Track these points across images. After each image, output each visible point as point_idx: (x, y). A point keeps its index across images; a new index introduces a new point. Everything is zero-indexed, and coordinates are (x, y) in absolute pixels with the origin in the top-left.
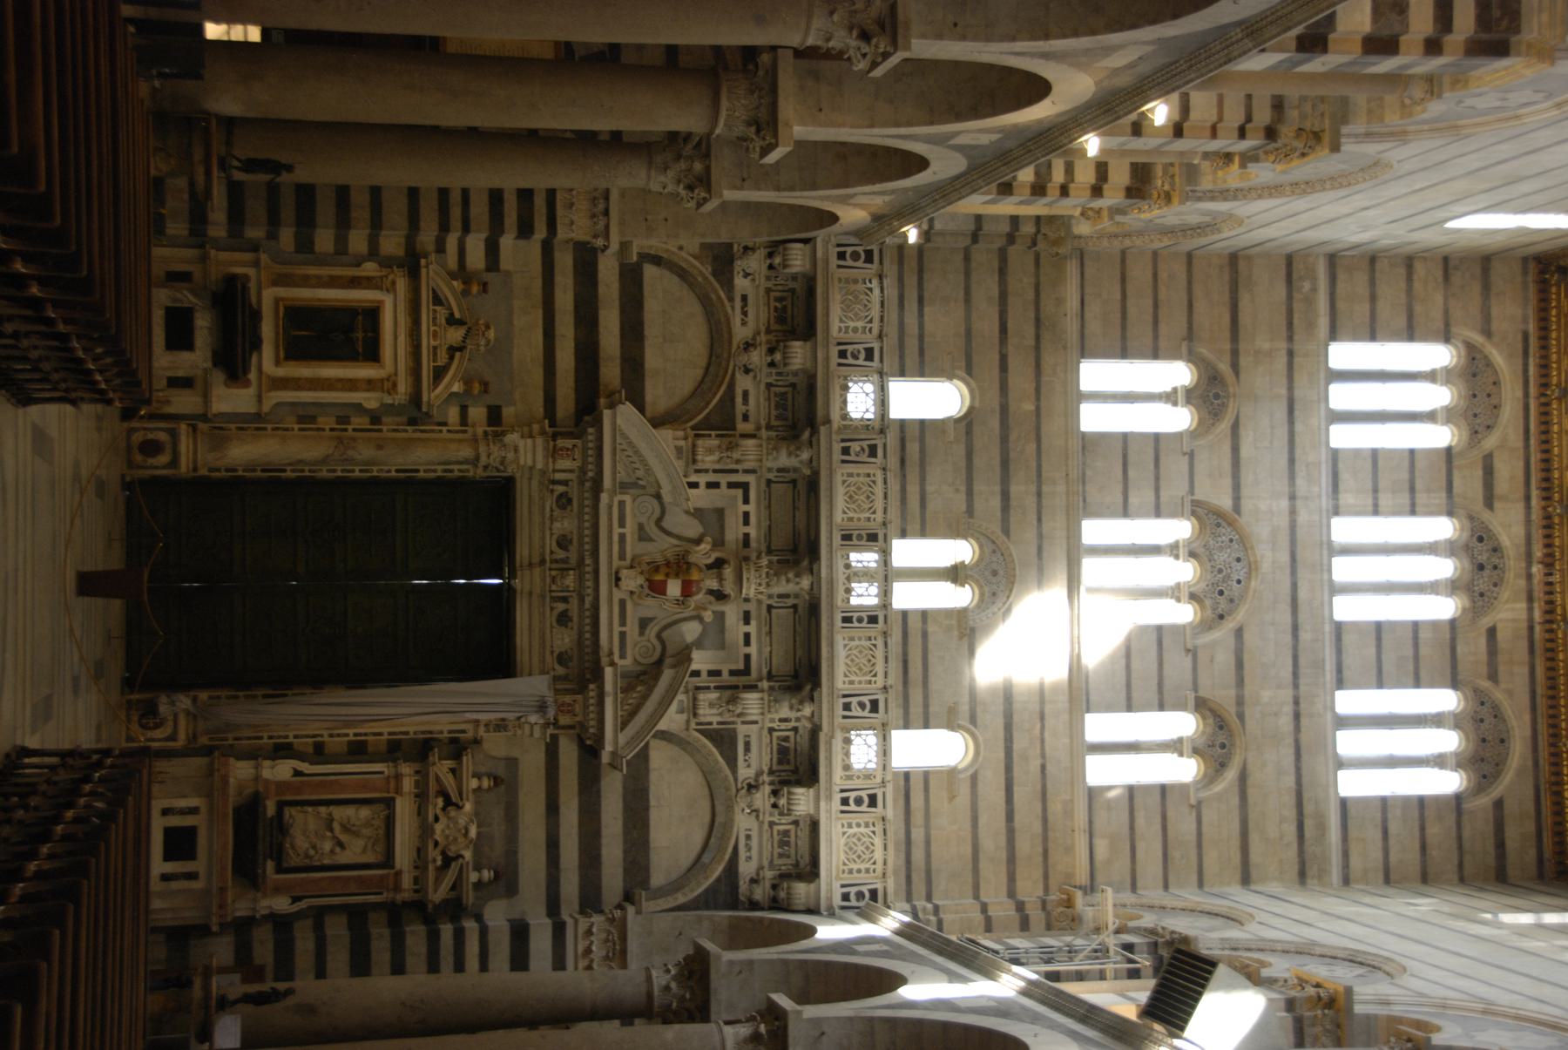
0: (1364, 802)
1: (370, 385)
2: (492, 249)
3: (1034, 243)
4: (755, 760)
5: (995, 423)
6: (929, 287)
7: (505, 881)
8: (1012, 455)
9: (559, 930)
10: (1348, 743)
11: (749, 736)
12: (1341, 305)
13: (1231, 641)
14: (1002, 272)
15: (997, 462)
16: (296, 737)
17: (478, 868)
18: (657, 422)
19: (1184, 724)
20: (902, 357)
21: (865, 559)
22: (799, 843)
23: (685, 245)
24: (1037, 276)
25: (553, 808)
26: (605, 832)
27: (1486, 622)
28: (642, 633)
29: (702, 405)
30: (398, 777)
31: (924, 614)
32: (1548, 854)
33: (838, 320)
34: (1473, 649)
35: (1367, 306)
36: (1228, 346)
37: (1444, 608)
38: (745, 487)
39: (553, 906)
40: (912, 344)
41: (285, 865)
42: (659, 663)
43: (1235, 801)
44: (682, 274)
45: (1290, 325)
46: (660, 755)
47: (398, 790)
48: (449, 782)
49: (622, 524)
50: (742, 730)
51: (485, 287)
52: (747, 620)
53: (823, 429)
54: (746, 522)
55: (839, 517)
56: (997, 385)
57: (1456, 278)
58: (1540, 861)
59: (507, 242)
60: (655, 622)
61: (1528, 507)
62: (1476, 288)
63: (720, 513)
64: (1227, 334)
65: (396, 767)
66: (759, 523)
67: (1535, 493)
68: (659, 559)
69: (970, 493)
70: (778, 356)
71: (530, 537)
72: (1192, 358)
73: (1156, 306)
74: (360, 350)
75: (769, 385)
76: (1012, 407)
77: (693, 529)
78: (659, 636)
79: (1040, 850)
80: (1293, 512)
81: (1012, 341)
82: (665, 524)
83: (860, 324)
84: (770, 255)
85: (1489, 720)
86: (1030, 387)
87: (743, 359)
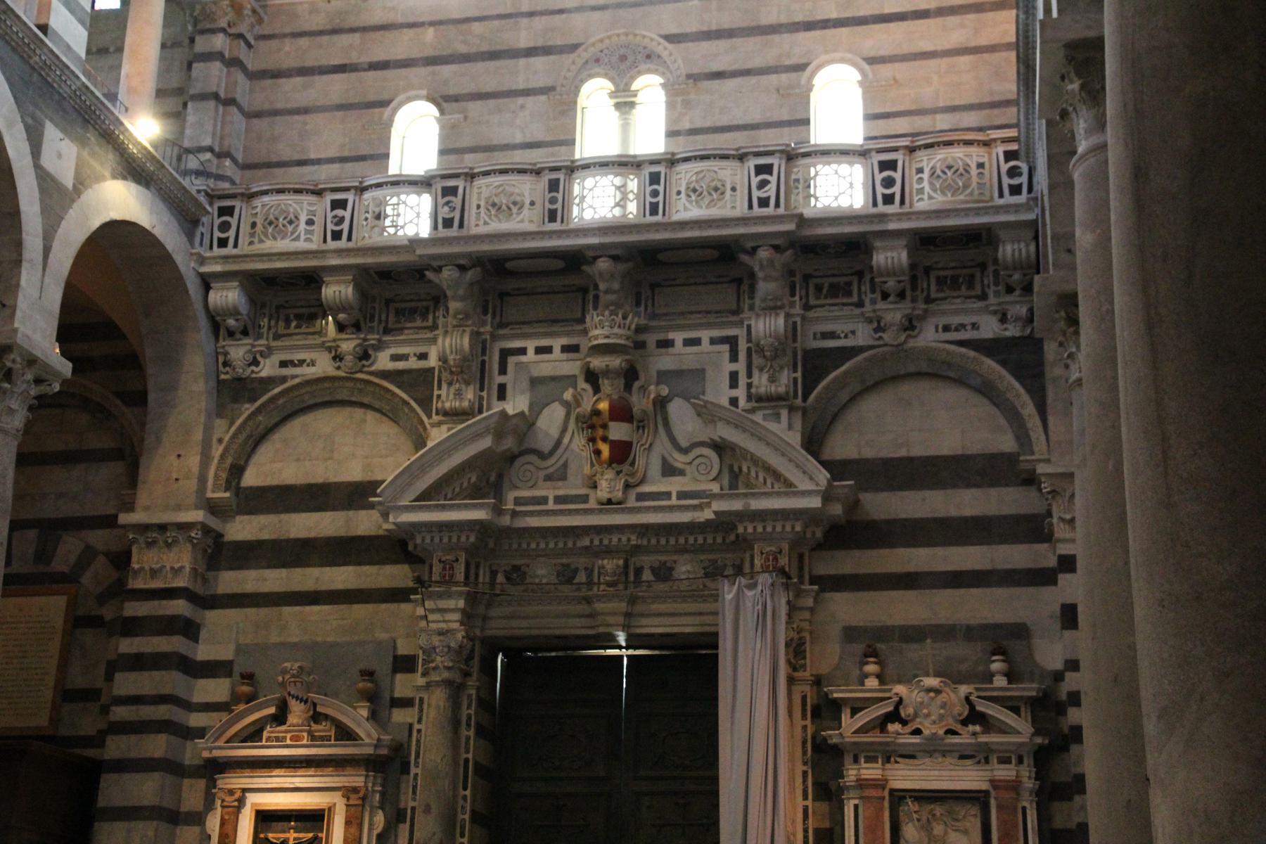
5: (446, 70)
6: (287, 154)
11: (815, 334)
15: (492, 65)
22: (952, 264)
26: (941, 512)
28: (682, 473)
29: (406, 410)
30: (862, 784)
47: (880, 784)
49: (544, 500)
51: (248, 677)
52: (666, 344)
54: (548, 350)
56: (403, 72)
59: (204, 652)
60: (667, 456)
65: (848, 788)
68: (587, 453)
69: (527, 93)
71: (558, 616)
74: (311, 835)
75: (387, 331)
76: (430, 52)
78: (685, 451)
81: (354, 58)
82: (546, 449)
86: (408, 34)
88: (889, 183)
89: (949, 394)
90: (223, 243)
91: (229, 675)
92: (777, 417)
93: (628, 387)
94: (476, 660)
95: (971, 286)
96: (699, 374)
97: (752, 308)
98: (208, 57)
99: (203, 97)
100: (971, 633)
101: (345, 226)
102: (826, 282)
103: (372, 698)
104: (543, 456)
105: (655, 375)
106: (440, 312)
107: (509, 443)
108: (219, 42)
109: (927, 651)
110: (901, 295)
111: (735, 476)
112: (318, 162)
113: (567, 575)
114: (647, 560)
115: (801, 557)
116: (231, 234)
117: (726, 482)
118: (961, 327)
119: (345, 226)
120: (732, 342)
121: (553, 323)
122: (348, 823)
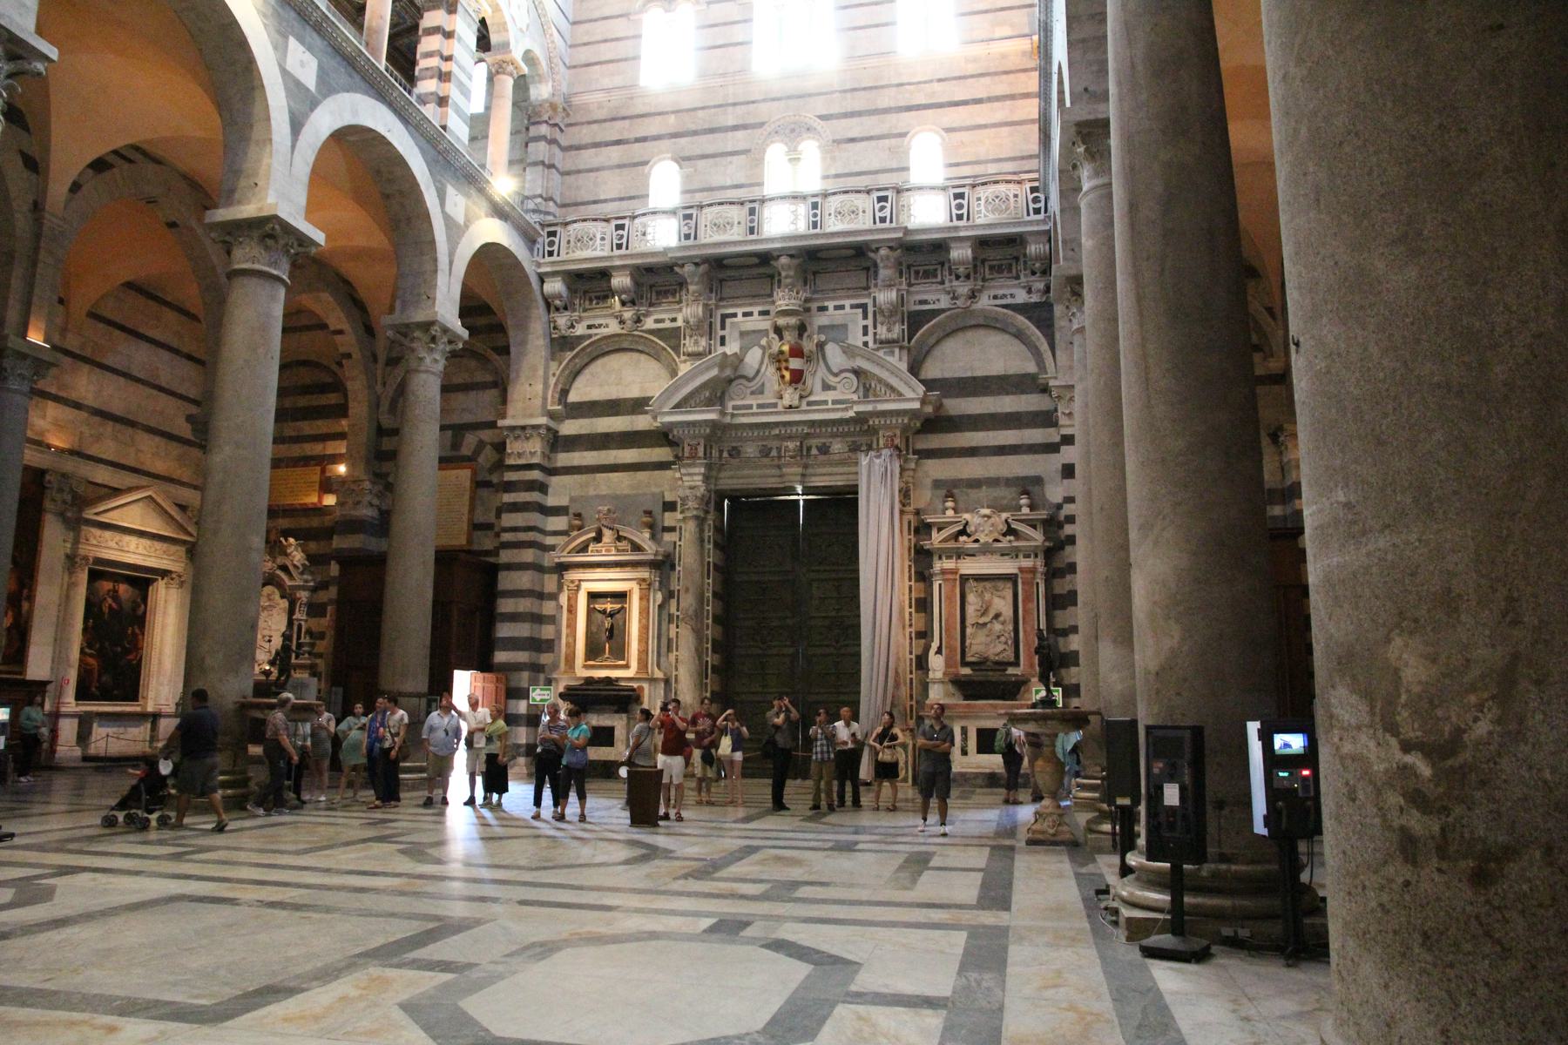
1: (644, 598)
3: (556, 125)
4: (935, 297)
5: (683, 141)
7: (1029, 486)
8: (706, 126)
14: (578, 148)
15: (710, 136)
16: (911, 653)
24: (582, 124)
26: (992, 410)
30: (944, 572)
41: (1012, 659)
46: (932, 370)
47: (954, 572)
48: (945, 533)
49: (750, 407)
51: (578, 515)
52: (823, 309)
59: (551, 501)
66: (751, 305)
68: (776, 378)
73: (606, 41)
75: (651, 305)
76: (672, 130)
78: (836, 375)
79: (1004, 77)
81: (626, 136)
88: (960, 207)
89: (995, 338)
90: (551, 254)
91: (567, 514)
92: (892, 353)
93: (801, 336)
94: (713, 503)
95: (1010, 270)
96: (844, 327)
97: (876, 285)
98: (537, 139)
99: (535, 164)
100: (1009, 482)
101: (624, 241)
102: (921, 269)
103: (651, 526)
104: (749, 380)
105: (816, 327)
106: (684, 292)
107: (728, 372)
108: (544, 129)
109: (984, 493)
110: (968, 277)
111: (867, 390)
112: (605, 201)
113: (765, 453)
114: (814, 442)
115: (907, 440)
116: (555, 248)
117: (861, 394)
118: (1004, 296)
119: (624, 241)
120: (864, 307)
121: (754, 297)
122: (641, 599)
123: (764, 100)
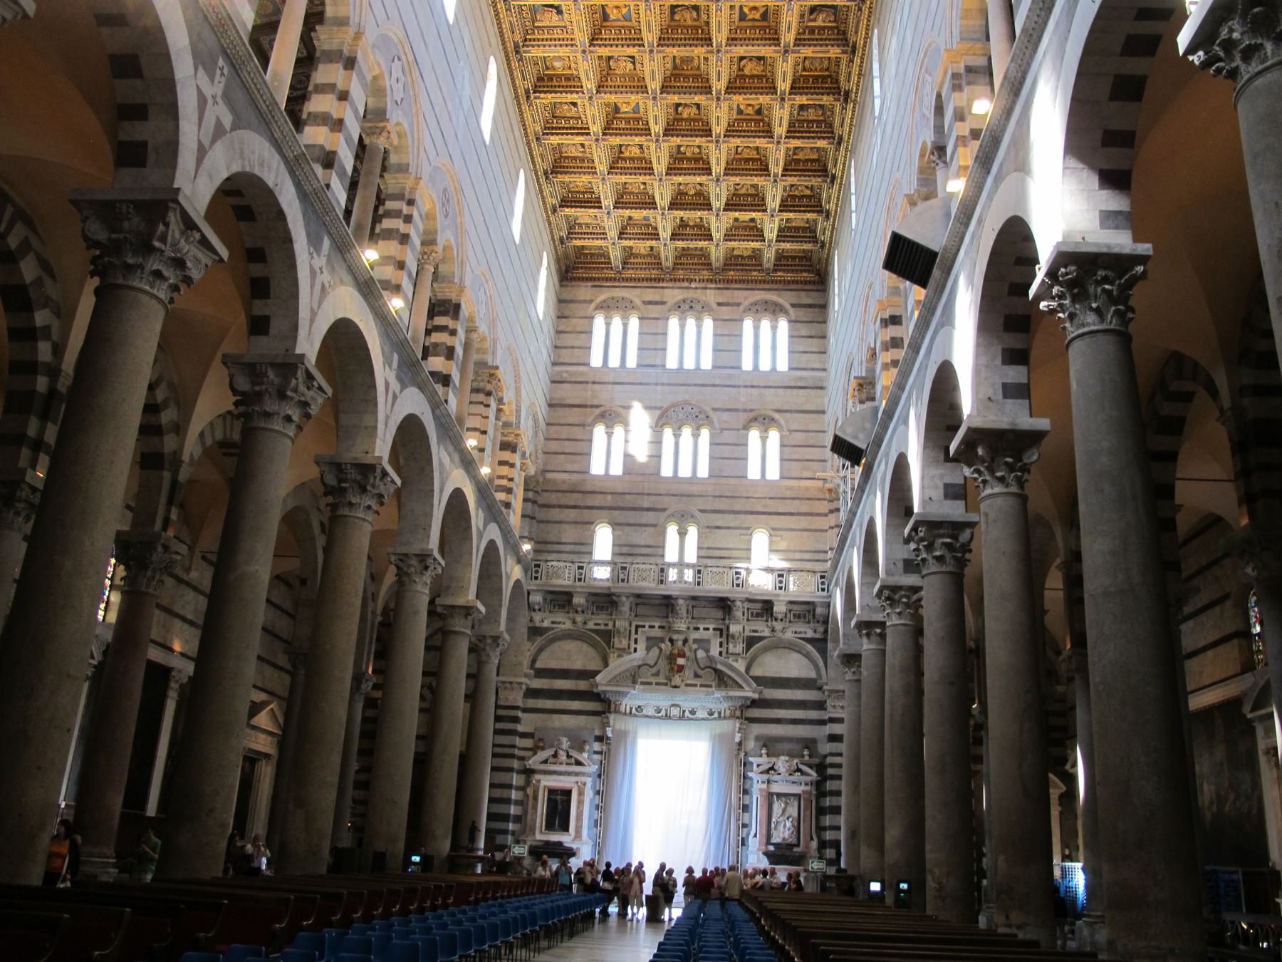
0: (790, 360)
2: (524, 735)
3: (537, 492)
4: (762, 628)
5: (616, 513)
7: (810, 744)
8: (631, 505)
9: (832, 720)
10: (765, 366)
12: (574, 361)
13: (719, 413)
14: (549, 506)
17: (803, 756)
18: (606, 665)
19: (754, 435)
20: (583, 553)
21: (672, 575)
23: (528, 649)
24: (552, 491)
25: (778, 721)
27: (715, 306)
31: (699, 548)
32: (814, 288)
33: (564, 581)
34: (726, 312)
35: (576, 350)
36: (589, 409)
37: (708, 323)
38: (637, 627)
39: (822, 722)
40: (578, 548)
42: (715, 670)
43: (788, 415)
44: (540, 650)
45: (581, 382)
46: (757, 671)
50: (747, 633)
52: (697, 629)
53: (613, 590)
55: (653, 585)
57: (567, 313)
58: (817, 290)
61: (667, 288)
62: (572, 305)
63: (648, 639)
64: (583, 409)
67: (661, 285)
69: (646, 525)
70: (579, 609)
72: (593, 425)
73: (569, 440)
75: (592, 614)
77: (655, 651)
78: (703, 669)
80: (663, 384)
81: (580, 503)
82: (652, 664)
83: (567, 571)
84: (534, 610)
85: (757, 307)
86: (601, 496)
87: (580, 625)
92: (737, 661)
96: (708, 641)
120: (721, 630)
123: (667, 495)
